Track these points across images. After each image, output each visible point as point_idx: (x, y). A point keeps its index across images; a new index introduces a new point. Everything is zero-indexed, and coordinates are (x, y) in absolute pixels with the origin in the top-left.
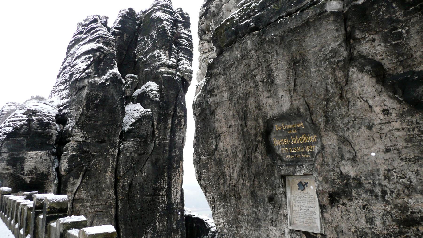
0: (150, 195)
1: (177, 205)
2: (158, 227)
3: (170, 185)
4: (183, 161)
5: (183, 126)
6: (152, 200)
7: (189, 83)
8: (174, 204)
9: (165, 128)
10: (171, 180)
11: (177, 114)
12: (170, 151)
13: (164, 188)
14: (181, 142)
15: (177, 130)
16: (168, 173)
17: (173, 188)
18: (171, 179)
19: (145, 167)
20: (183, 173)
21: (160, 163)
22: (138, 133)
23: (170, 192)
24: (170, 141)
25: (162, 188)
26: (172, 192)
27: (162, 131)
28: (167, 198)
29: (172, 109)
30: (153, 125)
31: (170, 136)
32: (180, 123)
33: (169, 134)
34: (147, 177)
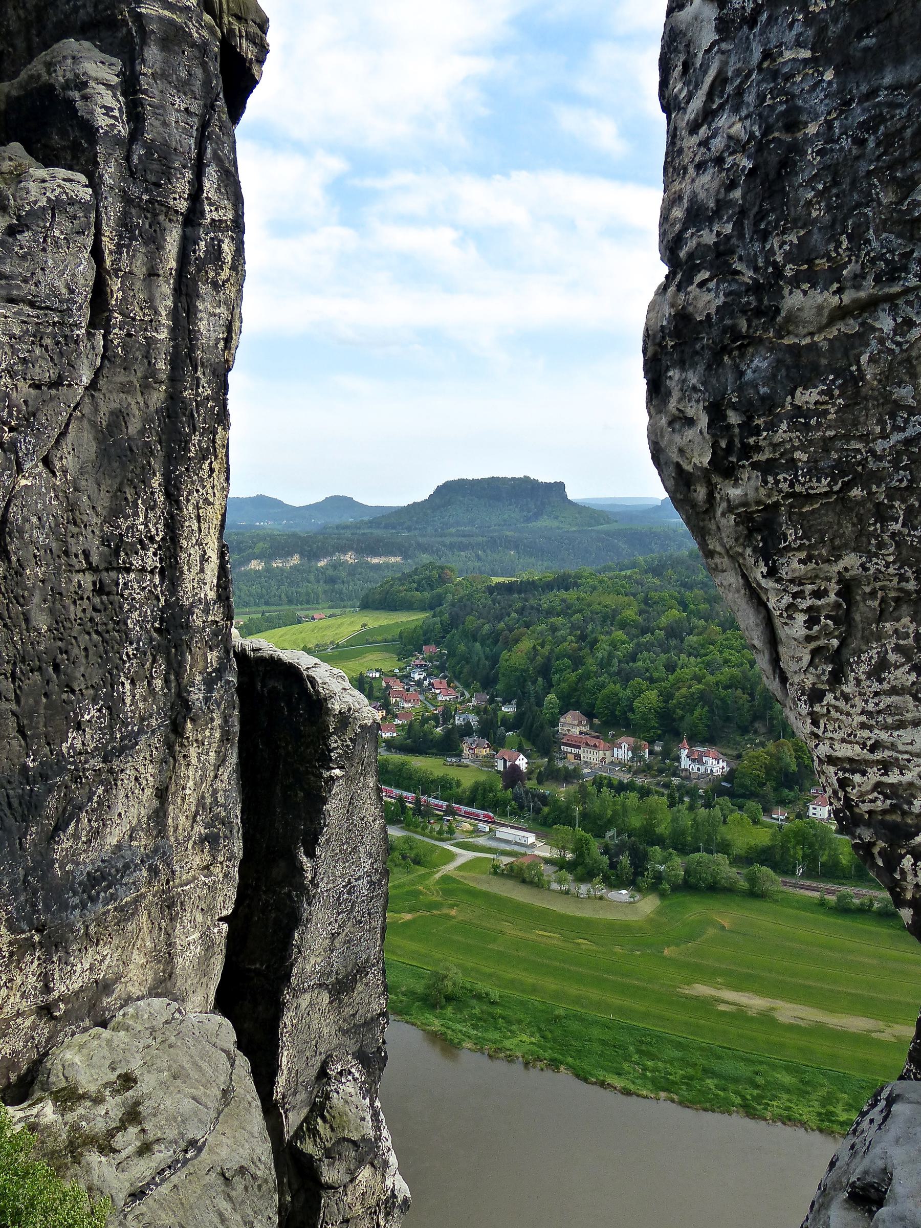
0: (91, 568)
1: (207, 611)
2: (128, 701)
3: (173, 526)
4: (227, 427)
5: (226, 272)
6: (100, 589)
7: (255, 69)
8: (192, 605)
9: (152, 274)
10: (180, 509)
11: (202, 214)
12: (175, 379)
13: (152, 539)
14: (221, 345)
15: (204, 289)
16: (167, 477)
17: (188, 539)
18: (178, 502)
19: (66, 447)
20: (227, 479)
21: (134, 427)
22: (25, 281)
23: (175, 556)
24: (174, 332)
25: (141, 542)
26: (183, 555)
27: (138, 285)
28: (162, 581)
29: (182, 185)
30: (97, 253)
31: (174, 314)
32: (215, 254)
33: (169, 303)
34: (76, 489)
